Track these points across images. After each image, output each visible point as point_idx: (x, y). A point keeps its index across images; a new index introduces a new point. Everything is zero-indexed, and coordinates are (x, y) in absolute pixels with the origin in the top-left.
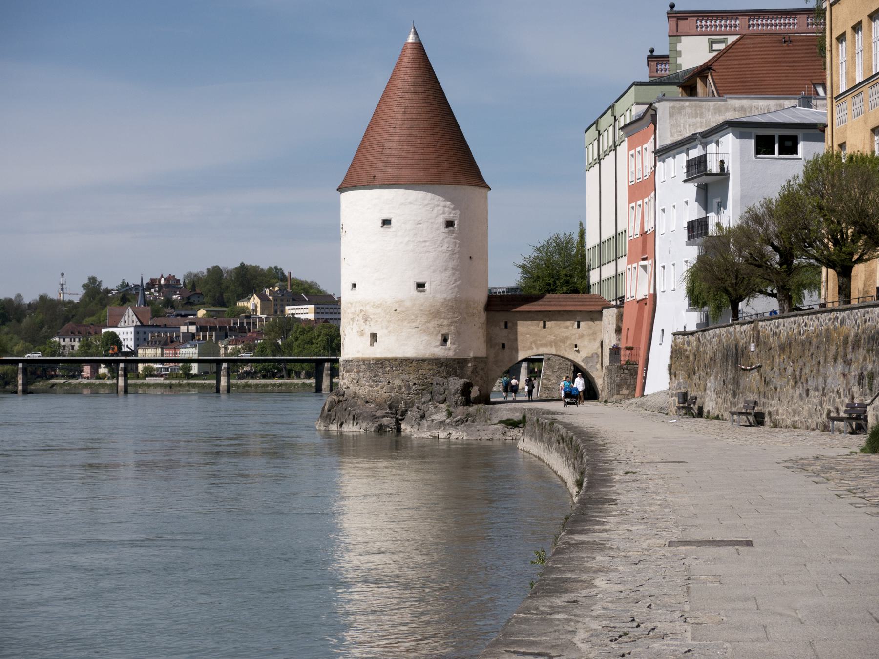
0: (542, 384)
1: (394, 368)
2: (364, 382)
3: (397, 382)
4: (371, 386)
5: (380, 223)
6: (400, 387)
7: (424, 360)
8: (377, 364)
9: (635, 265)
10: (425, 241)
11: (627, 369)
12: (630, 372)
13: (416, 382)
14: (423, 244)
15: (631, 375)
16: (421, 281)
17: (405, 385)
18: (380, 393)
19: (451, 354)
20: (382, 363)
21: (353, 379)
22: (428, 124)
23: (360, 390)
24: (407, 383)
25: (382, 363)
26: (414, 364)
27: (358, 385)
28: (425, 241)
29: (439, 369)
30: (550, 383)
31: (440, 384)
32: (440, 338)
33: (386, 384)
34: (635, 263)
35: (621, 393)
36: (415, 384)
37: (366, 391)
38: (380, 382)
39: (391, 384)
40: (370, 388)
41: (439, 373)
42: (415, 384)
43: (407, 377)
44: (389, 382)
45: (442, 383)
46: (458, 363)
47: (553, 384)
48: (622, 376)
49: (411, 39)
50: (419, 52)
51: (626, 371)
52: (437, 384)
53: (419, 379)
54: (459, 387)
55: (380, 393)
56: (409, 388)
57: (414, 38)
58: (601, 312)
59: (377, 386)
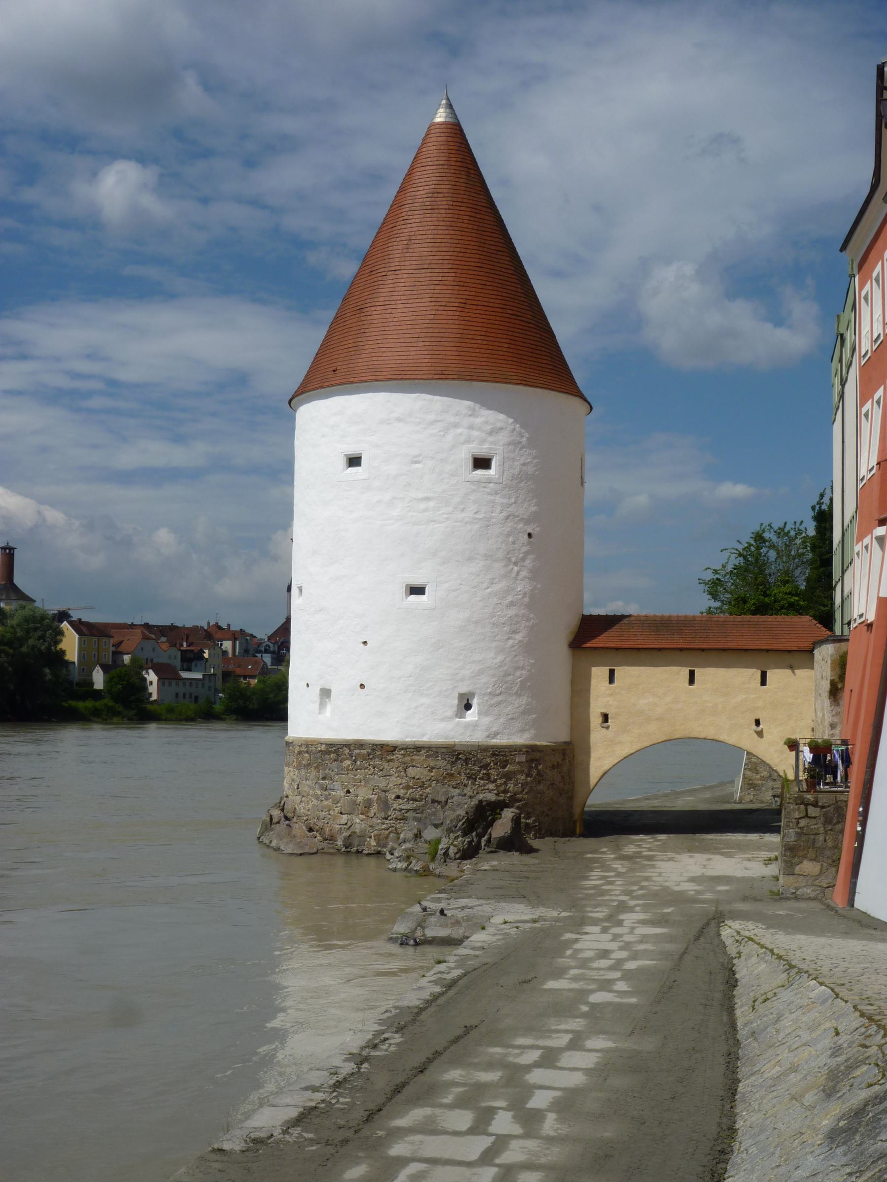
0: (744, 778)
1: (358, 763)
2: (306, 789)
3: (363, 794)
4: (317, 797)
5: (343, 462)
6: (368, 804)
7: (417, 748)
8: (329, 753)
9: (867, 540)
10: (427, 499)
11: (815, 804)
12: (825, 815)
13: (402, 792)
14: (423, 506)
15: (828, 821)
16: (417, 582)
17: (379, 798)
18: (332, 812)
19: (478, 737)
20: (335, 752)
21: (293, 780)
22: (450, 266)
23: (303, 804)
24: (382, 794)
25: (335, 752)
26: (398, 755)
27: (299, 793)
28: (427, 499)
29: (449, 766)
30: (758, 776)
31: (439, 802)
32: (456, 702)
33: (343, 794)
34: (868, 534)
35: (797, 869)
36: (398, 797)
37: (310, 806)
38: (333, 790)
39: (351, 796)
40: (315, 802)
41: (452, 775)
42: (398, 797)
43: (382, 784)
44: (348, 792)
45: (443, 799)
46: (494, 755)
47: (762, 778)
48: (803, 823)
49: (441, 116)
50: (450, 139)
51: (812, 811)
52: (434, 801)
53: (408, 787)
54: (463, 813)
55: (332, 812)
56: (385, 805)
57: (444, 115)
58: (811, 652)
59: (327, 799)
